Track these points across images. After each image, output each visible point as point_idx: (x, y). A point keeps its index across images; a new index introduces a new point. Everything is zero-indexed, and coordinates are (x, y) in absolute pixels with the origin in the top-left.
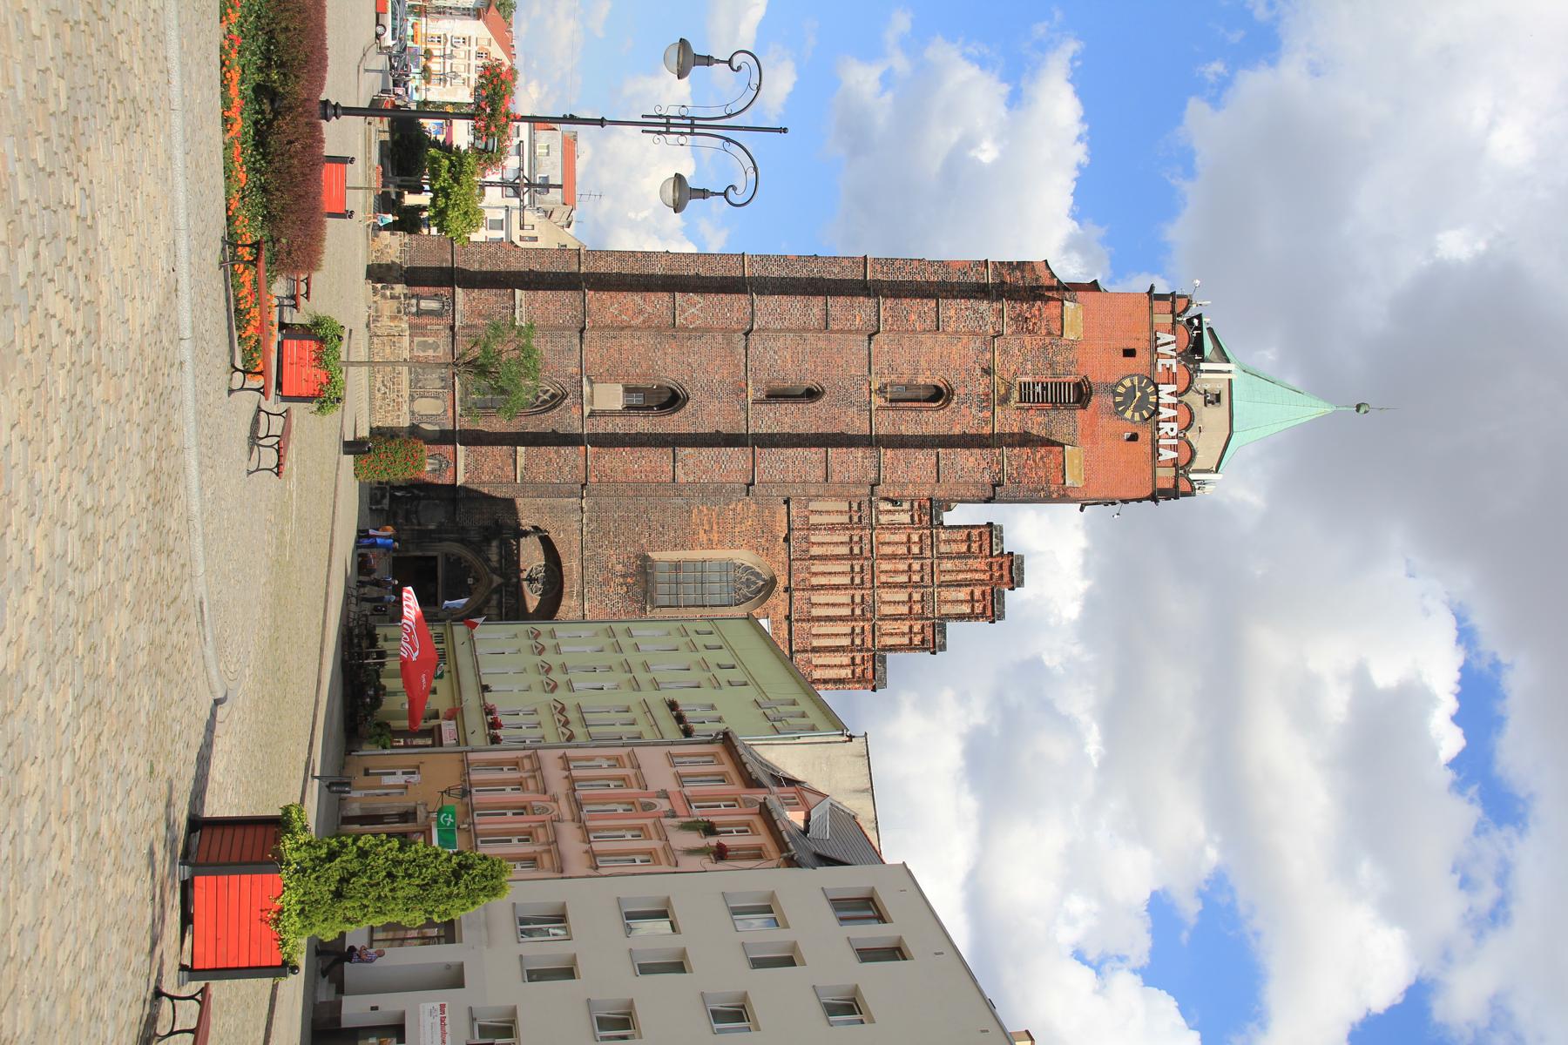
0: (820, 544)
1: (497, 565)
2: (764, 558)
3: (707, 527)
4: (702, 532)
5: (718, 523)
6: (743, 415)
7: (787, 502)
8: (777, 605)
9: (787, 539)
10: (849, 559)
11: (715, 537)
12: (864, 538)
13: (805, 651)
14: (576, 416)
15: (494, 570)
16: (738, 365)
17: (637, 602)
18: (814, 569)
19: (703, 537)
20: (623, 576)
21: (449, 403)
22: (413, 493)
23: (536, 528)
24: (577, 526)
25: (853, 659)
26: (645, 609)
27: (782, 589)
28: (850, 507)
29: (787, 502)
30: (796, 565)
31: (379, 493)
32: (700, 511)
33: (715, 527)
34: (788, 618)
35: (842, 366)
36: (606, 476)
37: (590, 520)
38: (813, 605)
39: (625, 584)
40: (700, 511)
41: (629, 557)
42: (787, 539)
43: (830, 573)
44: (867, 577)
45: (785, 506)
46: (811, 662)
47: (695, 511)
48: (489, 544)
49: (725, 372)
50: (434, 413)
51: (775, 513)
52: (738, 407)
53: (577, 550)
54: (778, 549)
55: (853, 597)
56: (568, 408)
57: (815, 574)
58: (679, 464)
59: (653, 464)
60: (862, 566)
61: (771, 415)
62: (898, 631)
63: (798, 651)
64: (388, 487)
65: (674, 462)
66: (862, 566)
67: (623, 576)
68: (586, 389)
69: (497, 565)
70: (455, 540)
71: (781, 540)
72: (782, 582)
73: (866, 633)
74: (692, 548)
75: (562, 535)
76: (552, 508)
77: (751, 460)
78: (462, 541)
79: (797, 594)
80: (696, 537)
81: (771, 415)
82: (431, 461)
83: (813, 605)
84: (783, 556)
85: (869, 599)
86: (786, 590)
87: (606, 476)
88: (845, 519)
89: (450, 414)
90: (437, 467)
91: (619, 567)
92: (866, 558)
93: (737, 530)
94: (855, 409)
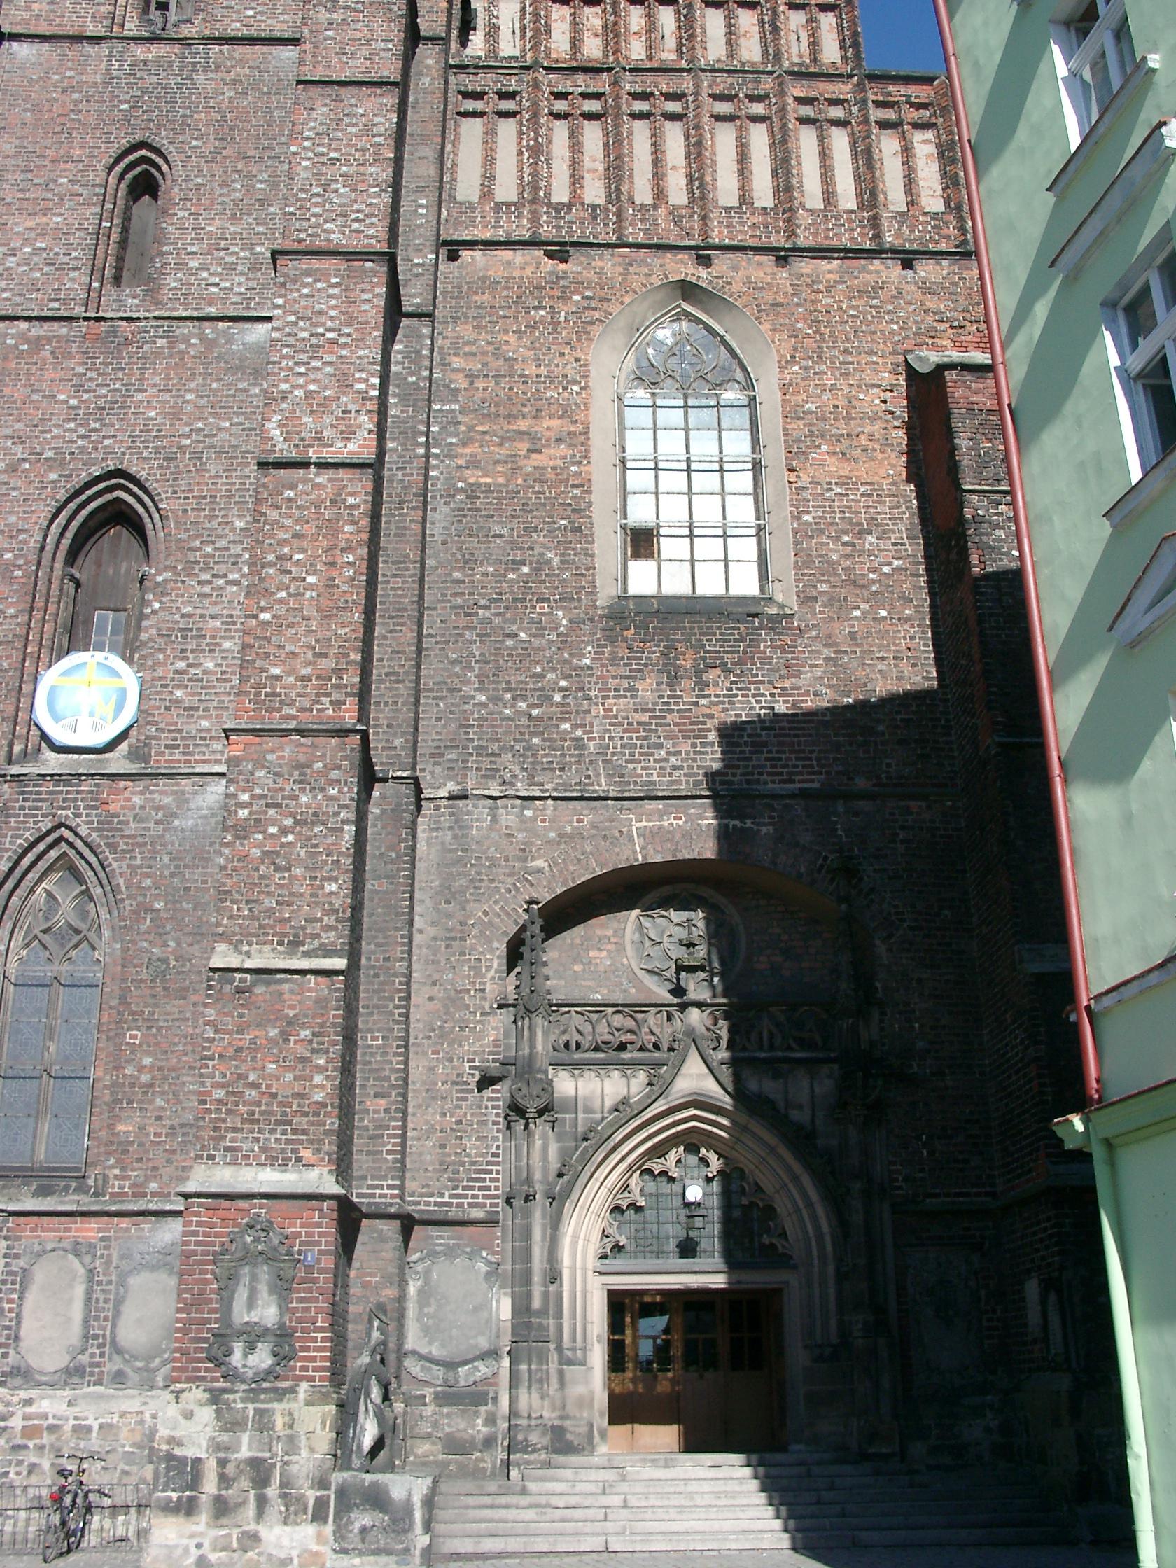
0: (576, 179)
1: (642, 1076)
2: (615, 309)
3: (522, 447)
4: (536, 459)
5: (510, 417)
6: (185, 329)
7: (453, 249)
8: (748, 282)
9: (559, 251)
10: (617, 126)
11: (550, 425)
12: (560, 88)
13: (875, 222)
14: (137, 800)
15: (659, 1087)
16: (37, 344)
17: (756, 640)
18: (644, 195)
19: (551, 457)
20: (674, 678)
21: (49, 1232)
22: (366, 1372)
23: (515, 953)
24: (508, 816)
25: (884, 125)
26: (772, 618)
27: (703, 273)
28: (475, 114)
29: (453, 249)
30: (634, 234)
31: (362, 1519)
32: (473, 463)
33: (523, 425)
34: (783, 258)
35: (76, 102)
36: (338, 672)
37: (491, 774)
38: (745, 198)
39: (698, 673)
40: (473, 463)
41: (614, 661)
42: (559, 251)
43: (656, 163)
44: (664, 84)
45: (466, 254)
46: (902, 214)
47: (473, 476)
48: (572, 1104)
49: (49, 374)
50: (80, 1290)
51: (484, 279)
52: (160, 342)
53: (588, 815)
54: (590, 275)
55: (718, 118)
56: (108, 824)
57: (660, 195)
58: (312, 454)
59: (310, 529)
60: (635, 96)
61: (194, 264)
62: (804, 35)
63: (877, 236)
64: (337, 1478)
65: (305, 465)
66: (635, 96)
67: (674, 678)
68: (52, 762)
69: (642, 1076)
70: (555, 1223)
71: (562, 266)
72: (684, 268)
73: (813, 94)
74: (585, 485)
75: (540, 863)
76: (448, 894)
77: (316, 264)
78: (558, 1200)
79: (718, 235)
80: (550, 475)
81: (194, 264)
82: (242, 1294)
83: (745, 198)
84: (608, 263)
85: (723, 83)
86: (706, 261)
87: (338, 672)
88: (507, 129)
89: (91, 1230)
90: (264, 1272)
91: (647, 689)
92: (615, 84)
93: (531, 370)
94: (200, 77)
